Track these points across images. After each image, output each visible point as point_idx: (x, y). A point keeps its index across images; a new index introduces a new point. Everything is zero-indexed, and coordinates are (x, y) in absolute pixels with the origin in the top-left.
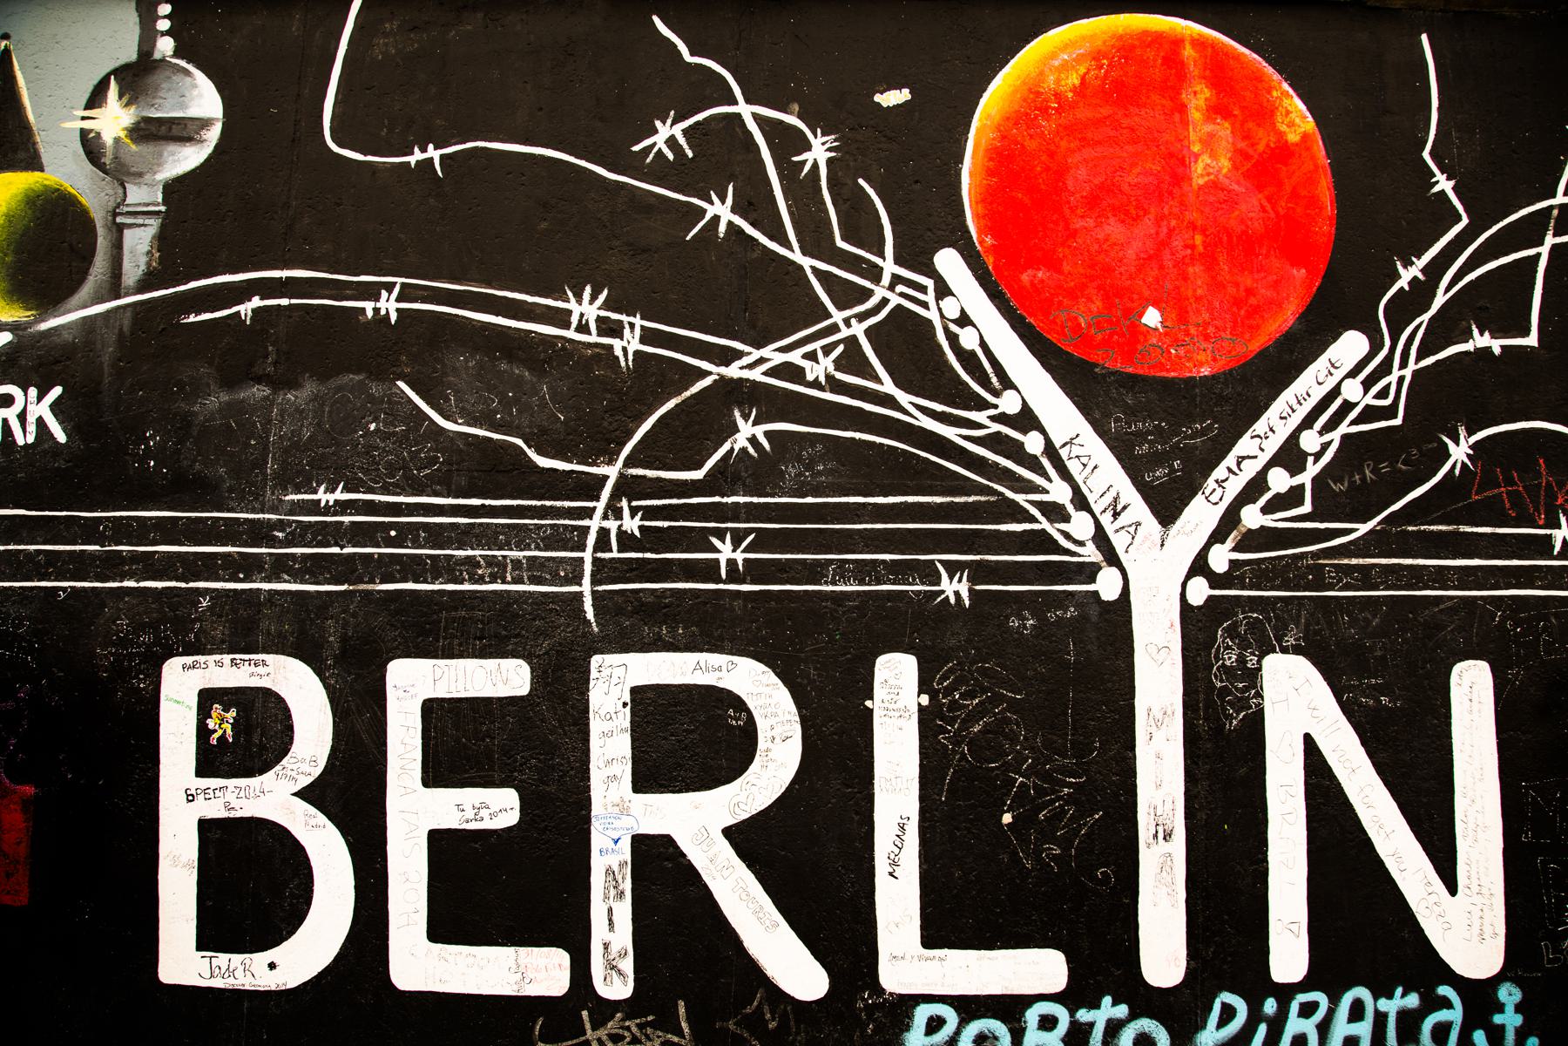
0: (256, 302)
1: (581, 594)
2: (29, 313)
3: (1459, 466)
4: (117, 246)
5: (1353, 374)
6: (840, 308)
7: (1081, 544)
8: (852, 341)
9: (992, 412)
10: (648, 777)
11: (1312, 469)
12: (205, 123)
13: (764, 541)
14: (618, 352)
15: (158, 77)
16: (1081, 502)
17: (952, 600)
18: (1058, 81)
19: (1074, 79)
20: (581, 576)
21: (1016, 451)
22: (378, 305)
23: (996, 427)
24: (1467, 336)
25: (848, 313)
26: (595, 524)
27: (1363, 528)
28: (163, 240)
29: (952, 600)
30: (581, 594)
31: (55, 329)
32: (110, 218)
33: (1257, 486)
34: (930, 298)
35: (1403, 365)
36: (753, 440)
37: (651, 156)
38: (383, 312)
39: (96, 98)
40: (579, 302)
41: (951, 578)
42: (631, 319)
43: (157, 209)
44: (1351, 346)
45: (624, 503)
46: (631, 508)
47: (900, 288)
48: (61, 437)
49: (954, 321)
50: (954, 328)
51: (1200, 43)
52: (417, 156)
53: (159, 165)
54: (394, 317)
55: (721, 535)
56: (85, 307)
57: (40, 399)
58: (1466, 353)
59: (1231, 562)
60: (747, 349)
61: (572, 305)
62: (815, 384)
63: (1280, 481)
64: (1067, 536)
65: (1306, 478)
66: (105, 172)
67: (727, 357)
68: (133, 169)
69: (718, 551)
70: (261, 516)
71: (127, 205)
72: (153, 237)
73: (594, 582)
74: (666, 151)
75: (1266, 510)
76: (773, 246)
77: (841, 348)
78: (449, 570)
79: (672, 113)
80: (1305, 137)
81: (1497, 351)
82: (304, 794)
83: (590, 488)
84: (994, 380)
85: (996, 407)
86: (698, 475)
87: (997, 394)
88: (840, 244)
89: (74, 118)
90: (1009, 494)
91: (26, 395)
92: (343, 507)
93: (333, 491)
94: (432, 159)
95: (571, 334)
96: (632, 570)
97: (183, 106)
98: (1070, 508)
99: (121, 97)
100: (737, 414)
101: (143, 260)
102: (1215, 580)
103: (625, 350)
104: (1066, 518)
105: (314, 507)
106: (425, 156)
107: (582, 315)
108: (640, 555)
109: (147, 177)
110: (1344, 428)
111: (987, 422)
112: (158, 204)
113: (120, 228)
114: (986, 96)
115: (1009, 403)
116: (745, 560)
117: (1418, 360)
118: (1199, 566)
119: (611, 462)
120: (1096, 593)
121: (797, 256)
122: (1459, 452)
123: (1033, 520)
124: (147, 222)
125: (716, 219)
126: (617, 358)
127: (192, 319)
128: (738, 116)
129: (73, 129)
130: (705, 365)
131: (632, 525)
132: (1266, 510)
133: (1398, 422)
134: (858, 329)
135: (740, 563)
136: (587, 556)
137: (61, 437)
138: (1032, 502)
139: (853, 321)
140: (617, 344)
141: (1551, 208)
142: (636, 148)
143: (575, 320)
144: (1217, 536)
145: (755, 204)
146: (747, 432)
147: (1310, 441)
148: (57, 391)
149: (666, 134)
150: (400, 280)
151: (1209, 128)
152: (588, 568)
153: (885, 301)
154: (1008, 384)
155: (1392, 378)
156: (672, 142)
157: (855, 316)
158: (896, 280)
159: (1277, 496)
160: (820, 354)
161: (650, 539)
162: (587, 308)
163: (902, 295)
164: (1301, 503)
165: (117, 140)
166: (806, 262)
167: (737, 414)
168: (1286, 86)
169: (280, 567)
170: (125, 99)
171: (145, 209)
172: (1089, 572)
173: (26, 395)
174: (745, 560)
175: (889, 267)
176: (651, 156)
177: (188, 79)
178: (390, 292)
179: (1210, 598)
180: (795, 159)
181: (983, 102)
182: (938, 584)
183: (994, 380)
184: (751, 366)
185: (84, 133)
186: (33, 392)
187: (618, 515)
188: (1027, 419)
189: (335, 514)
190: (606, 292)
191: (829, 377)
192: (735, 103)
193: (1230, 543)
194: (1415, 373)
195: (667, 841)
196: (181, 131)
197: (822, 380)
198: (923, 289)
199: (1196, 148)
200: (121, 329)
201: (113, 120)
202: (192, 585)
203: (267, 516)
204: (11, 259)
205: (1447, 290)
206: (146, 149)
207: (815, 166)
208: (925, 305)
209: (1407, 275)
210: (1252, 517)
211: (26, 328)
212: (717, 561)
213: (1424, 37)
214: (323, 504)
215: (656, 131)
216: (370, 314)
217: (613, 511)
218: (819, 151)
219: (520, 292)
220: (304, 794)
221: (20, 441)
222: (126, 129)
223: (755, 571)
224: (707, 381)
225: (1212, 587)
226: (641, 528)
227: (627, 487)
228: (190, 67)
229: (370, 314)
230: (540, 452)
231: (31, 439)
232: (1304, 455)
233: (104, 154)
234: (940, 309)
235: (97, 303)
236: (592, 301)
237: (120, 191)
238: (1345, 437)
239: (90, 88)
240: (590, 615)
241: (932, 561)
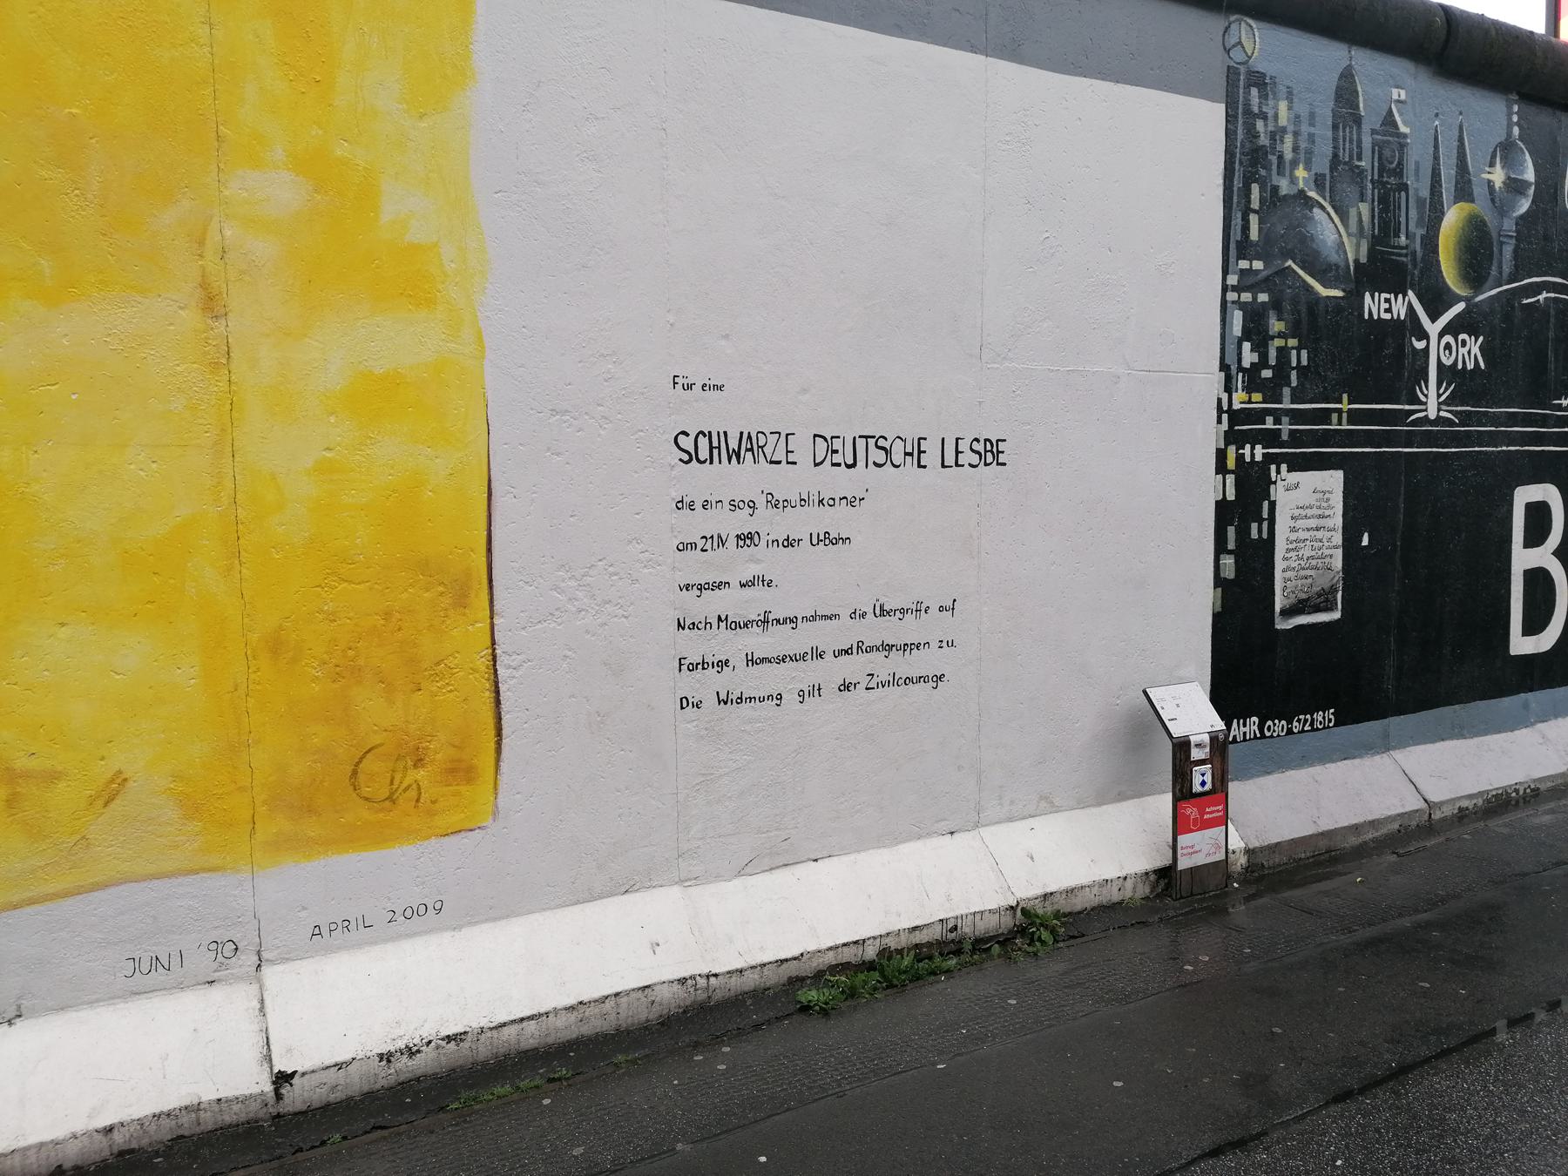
12: (1528, 184)
53: (1514, 207)
165: (1500, 187)
201: (1498, 176)
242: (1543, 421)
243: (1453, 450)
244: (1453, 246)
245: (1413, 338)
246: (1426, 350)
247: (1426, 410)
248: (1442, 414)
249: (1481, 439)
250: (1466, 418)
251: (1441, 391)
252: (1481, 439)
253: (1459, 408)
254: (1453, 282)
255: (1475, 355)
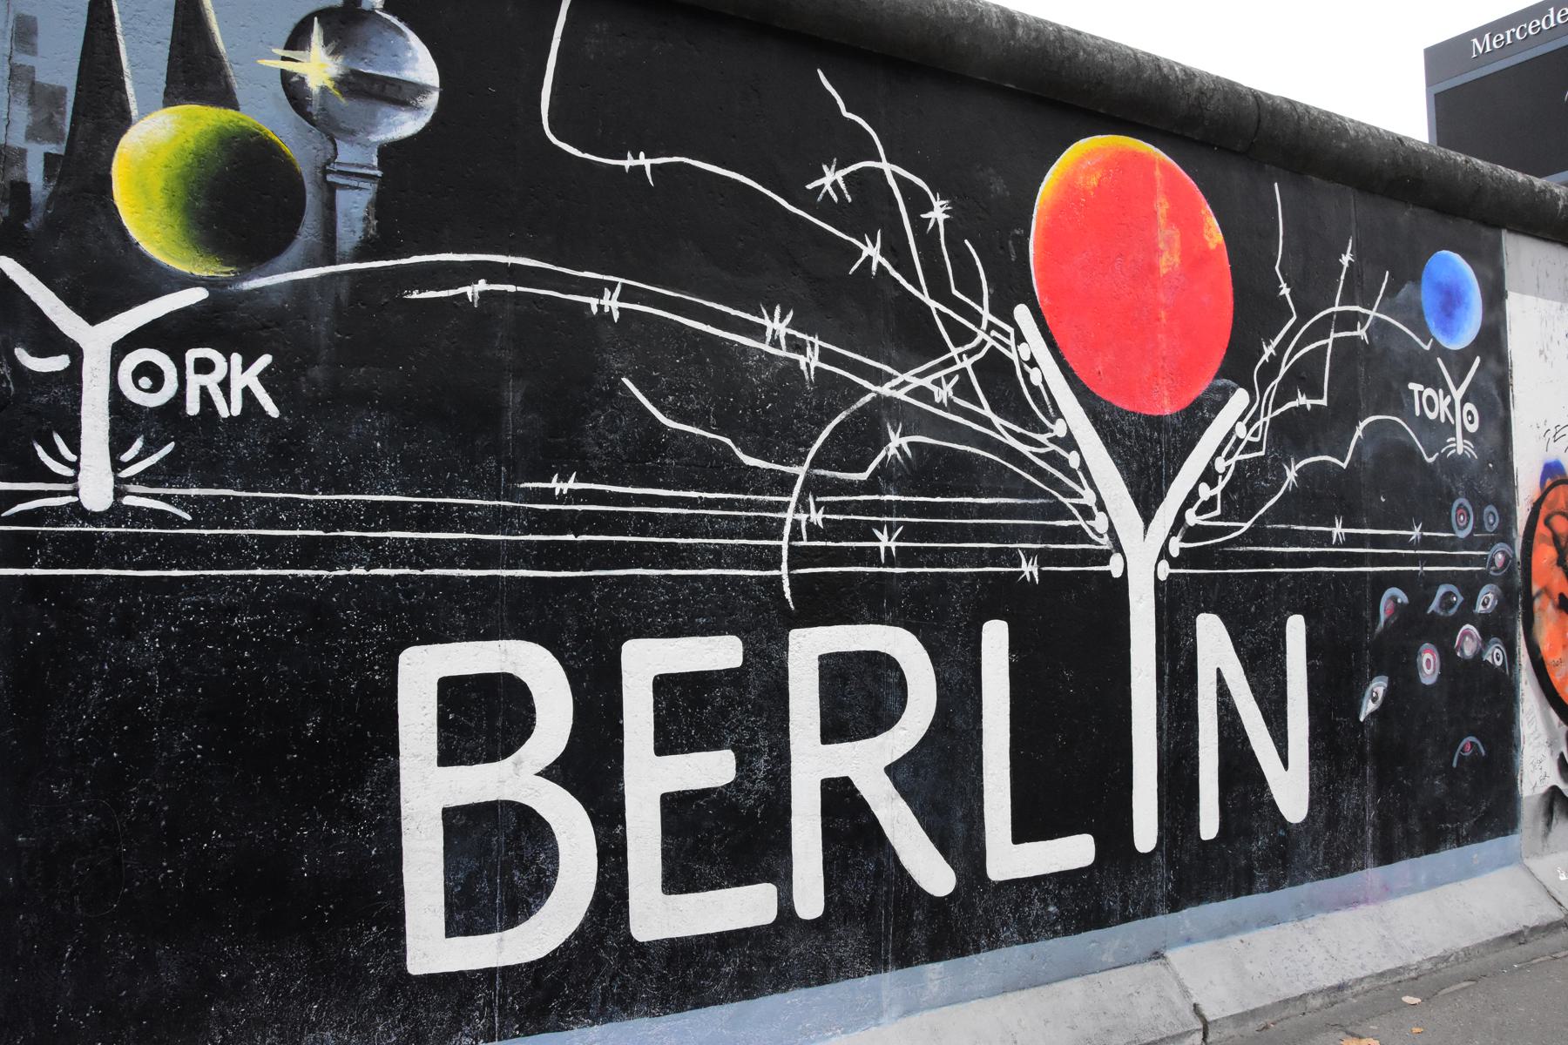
0: (482, 285)
1: (779, 578)
2: (229, 269)
3: (1291, 484)
4: (330, 206)
5: (1241, 419)
6: (956, 345)
7: (1101, 536)
8: (963, 372)
9: (1050, 435)
10: (833, 731)
11: (1222, 484)
12: (422, 90)
13: (910, 532)
14: (803, 367)
15: (366, 29)
16: (1101, 506)
17: (1029, 579)
18: (1085, 181)
19: (1094, 182)
20: (780, 562)
21: (1062, 464)
22: (602, 302)
23: (1052, 447)
24: (1295, 398)
25: (961, 349)
26: (789, 516)
27: (1246, 526)
28: (380, 206)
29: (1029, 579)
30: (779, 578)
31: (261, 290)
32: (320, 175)
33: (1193, 496)
34: (1011, 342)
35: (1266, 415)
36: (900, 449)
37: (821, 195)
38: (607, 310)
39: (298, 40)
40: (772, 318)
41: (1028, 562)
42: (811, 339)
43: (372, 172)
44: (1240, 398)
45: (811, 499)
46: (815, 502)
47: (993, 333)
48: (272, 410)
49: (1026, 362)
50: (1027, 367)
51: (1164, 166)
52: (628, 163)
54: (616, 316)
55: (880, 526)
56: (295, 269)
57: (245, 367)
58: (1295, 408)
59: (1181, 549)
60: (895, 373)
61: (766, 322)
62: (940, 406)
63: (1205, 492)
64: (1093, 529)
65: (1218, 491)
66: (312, 123)
67: (879, 378)
68: (343, 125)
69: (879, 541)
70: (496, 503)
71: (339, 164)
72: (370, 203)
73: (791, 567)
74: (832, 193)
75: (1198, 513)
76: (910, 288)
77: (956, 378)
78: (673, 556)
79: (835, 160)
80: (1218, 245)
81: (1309, 407)
82: (548, 773)
83: (785, 484)
84: (1051, 410)
85: (1052, 431)
86: (864, 476)
87: (1053, 422)
88: (955, 292)
89: (274, 57)
90: (1061, 498)
91: (228, 361)
92: (575, 496)
93: (566, 481)
94: (642, 168)
95: (766, 348)
96: (817, 557)
97: (398, 68)
98: (1095, 509)
99: (326, 42)
100: (889, 427)
101: (360, 226)
102: (1174, 563)
103: (808, 365)
104: (1093, 518)
105: (548, 496)
106: (636, 163)
107: (774, 331)
108: (823, 544)
109: (361, 135)
110: (1237, 457)
111: (1046, 442)
112: (373, 168)
113: (332, 188)
114: (1043, 184)
115: (1059, 429)
116: (897, 548)
117: (1273, 411)
118: (1164, 553)
119: (800, 463)
120: (1109, 572)
121: (926, 298)
122: (1291, 475)
123: (1075, 518)
124: (362, 185)
125: (869, 259)
126: (802, 372)
127: (415, 295)
128: (882, 171)
129: (272, 69)
130: (866, 384)
131: (817, 517)
132: (1198, 513)
133: (1262, 453)
134: (967, 363)
135: (894, 550)
136: (784, 544)
137: (272, 410)
138: (1073, 504)
139: (964, 356)
140: (802, 360)
141: (1333, 313)
142: (809, 187)
143: (769, 333)
144: (1174, 531)
145: (895, 250)
146: (897, 443)
147: (1220, 465)
148: (265, 360)
149: (831, 178)
150: (621, 280)
151: (1168, 232)
152: (785, 554)
153: (984, 343)
154: (1059, 415)
155: (1260, 423)
156: (835, 185)
157: (966, 352)
158: (991, 326)
159: (1204, 502)
160: (943, 380)
161: (832, 530)
162: (778, 325)
163: (995, 338)
164: (1214, 508)
165: (324, 90)
166: (933, 304)
167: (889, 427)
168: (1208, 207)
169: (517, 556)
170: (331, 47)
171: (359, 171)
172: (1104, 557)
173: (228, 361)
174: (897, 548)
175: (987, 316)
176: (821, 195)
177: (401, 38)
178: (612, 291)
179: (1171, 575)
180: (923, 216)
181: (1041, 189)
182: (1019, 565)
183: (1051, 410)
184: (897, 388)
185: (285, 76)
186: (236, 358)
187: (807, 511)
188: (1069, 442)
189: (569, 503)
190: (791, 313)
191: (950, 401)
192: (879, 160)
193: (1179, 537)
194: (1271, 419)
195: (847, 781)
196: (401, 94)
197: (945, 401)
198: (1007, 335)
199: (1161, 246)
200: (338, 298)
202: (427, 572)
203: (502, 503)
204: (203, 204)
205: (1286, 365)
206: (359, 106)
207: (936, 224)
208: (1007, 347)
209: (1269, 351)
210: (1192, 518)
211: (225, 286)
212: (878, 548)
213: (1276, 185)
214: (557, 492)
215: (823, 175)
216: (595, 310)
217: (803, 505)
218: (938, 213)
219: (725, 304)
220: (548, 773)
221: (223, 412)
222: (331, 79)
223: (905, 557)
224: (868, 398)
225: (1171, 567)
226: (823, 519)
227: (815, 486)
228: (402, 26)
229: (595, 310)
230: (745, 452)
231: (237, 409)
232: (1217, 474)
233: (309, 103)
234: (1018, 352)
235: (309, 267)
236: (781, 320)
237: (330, 147)
238: (1238, 462)
239: (291, 27)
240: (788, 595)
241: (1016, 549)
242: (499, 520)
243: (176, 573)
244: (161, 184)
245: (22, 355)
246: (73, 376)
247: (75, 493)
248: (128, 501)
249: (233, 551)
250: (204, 511)
251: (126, 457)
252: (233, 551)
253: (194, 492)
254: (161, 249)
255: (247, 392)
